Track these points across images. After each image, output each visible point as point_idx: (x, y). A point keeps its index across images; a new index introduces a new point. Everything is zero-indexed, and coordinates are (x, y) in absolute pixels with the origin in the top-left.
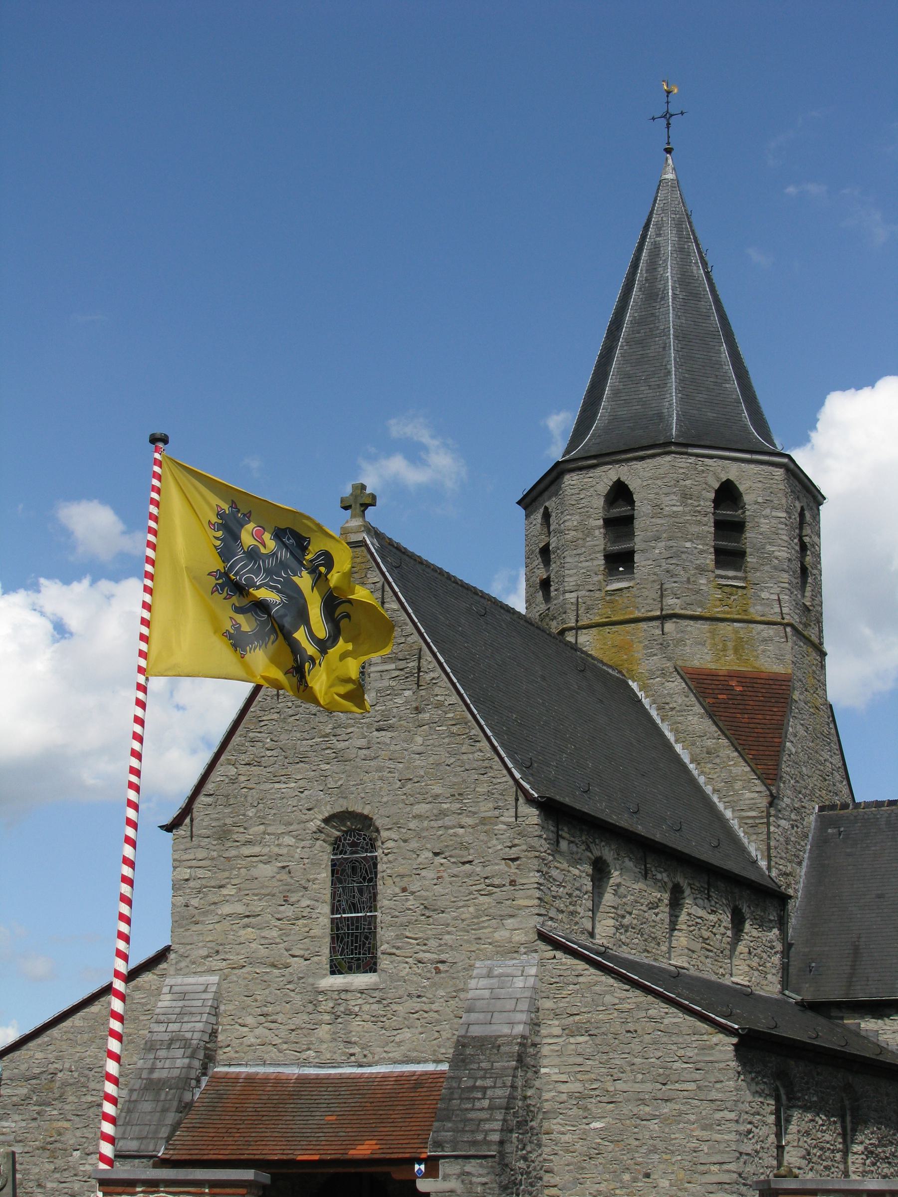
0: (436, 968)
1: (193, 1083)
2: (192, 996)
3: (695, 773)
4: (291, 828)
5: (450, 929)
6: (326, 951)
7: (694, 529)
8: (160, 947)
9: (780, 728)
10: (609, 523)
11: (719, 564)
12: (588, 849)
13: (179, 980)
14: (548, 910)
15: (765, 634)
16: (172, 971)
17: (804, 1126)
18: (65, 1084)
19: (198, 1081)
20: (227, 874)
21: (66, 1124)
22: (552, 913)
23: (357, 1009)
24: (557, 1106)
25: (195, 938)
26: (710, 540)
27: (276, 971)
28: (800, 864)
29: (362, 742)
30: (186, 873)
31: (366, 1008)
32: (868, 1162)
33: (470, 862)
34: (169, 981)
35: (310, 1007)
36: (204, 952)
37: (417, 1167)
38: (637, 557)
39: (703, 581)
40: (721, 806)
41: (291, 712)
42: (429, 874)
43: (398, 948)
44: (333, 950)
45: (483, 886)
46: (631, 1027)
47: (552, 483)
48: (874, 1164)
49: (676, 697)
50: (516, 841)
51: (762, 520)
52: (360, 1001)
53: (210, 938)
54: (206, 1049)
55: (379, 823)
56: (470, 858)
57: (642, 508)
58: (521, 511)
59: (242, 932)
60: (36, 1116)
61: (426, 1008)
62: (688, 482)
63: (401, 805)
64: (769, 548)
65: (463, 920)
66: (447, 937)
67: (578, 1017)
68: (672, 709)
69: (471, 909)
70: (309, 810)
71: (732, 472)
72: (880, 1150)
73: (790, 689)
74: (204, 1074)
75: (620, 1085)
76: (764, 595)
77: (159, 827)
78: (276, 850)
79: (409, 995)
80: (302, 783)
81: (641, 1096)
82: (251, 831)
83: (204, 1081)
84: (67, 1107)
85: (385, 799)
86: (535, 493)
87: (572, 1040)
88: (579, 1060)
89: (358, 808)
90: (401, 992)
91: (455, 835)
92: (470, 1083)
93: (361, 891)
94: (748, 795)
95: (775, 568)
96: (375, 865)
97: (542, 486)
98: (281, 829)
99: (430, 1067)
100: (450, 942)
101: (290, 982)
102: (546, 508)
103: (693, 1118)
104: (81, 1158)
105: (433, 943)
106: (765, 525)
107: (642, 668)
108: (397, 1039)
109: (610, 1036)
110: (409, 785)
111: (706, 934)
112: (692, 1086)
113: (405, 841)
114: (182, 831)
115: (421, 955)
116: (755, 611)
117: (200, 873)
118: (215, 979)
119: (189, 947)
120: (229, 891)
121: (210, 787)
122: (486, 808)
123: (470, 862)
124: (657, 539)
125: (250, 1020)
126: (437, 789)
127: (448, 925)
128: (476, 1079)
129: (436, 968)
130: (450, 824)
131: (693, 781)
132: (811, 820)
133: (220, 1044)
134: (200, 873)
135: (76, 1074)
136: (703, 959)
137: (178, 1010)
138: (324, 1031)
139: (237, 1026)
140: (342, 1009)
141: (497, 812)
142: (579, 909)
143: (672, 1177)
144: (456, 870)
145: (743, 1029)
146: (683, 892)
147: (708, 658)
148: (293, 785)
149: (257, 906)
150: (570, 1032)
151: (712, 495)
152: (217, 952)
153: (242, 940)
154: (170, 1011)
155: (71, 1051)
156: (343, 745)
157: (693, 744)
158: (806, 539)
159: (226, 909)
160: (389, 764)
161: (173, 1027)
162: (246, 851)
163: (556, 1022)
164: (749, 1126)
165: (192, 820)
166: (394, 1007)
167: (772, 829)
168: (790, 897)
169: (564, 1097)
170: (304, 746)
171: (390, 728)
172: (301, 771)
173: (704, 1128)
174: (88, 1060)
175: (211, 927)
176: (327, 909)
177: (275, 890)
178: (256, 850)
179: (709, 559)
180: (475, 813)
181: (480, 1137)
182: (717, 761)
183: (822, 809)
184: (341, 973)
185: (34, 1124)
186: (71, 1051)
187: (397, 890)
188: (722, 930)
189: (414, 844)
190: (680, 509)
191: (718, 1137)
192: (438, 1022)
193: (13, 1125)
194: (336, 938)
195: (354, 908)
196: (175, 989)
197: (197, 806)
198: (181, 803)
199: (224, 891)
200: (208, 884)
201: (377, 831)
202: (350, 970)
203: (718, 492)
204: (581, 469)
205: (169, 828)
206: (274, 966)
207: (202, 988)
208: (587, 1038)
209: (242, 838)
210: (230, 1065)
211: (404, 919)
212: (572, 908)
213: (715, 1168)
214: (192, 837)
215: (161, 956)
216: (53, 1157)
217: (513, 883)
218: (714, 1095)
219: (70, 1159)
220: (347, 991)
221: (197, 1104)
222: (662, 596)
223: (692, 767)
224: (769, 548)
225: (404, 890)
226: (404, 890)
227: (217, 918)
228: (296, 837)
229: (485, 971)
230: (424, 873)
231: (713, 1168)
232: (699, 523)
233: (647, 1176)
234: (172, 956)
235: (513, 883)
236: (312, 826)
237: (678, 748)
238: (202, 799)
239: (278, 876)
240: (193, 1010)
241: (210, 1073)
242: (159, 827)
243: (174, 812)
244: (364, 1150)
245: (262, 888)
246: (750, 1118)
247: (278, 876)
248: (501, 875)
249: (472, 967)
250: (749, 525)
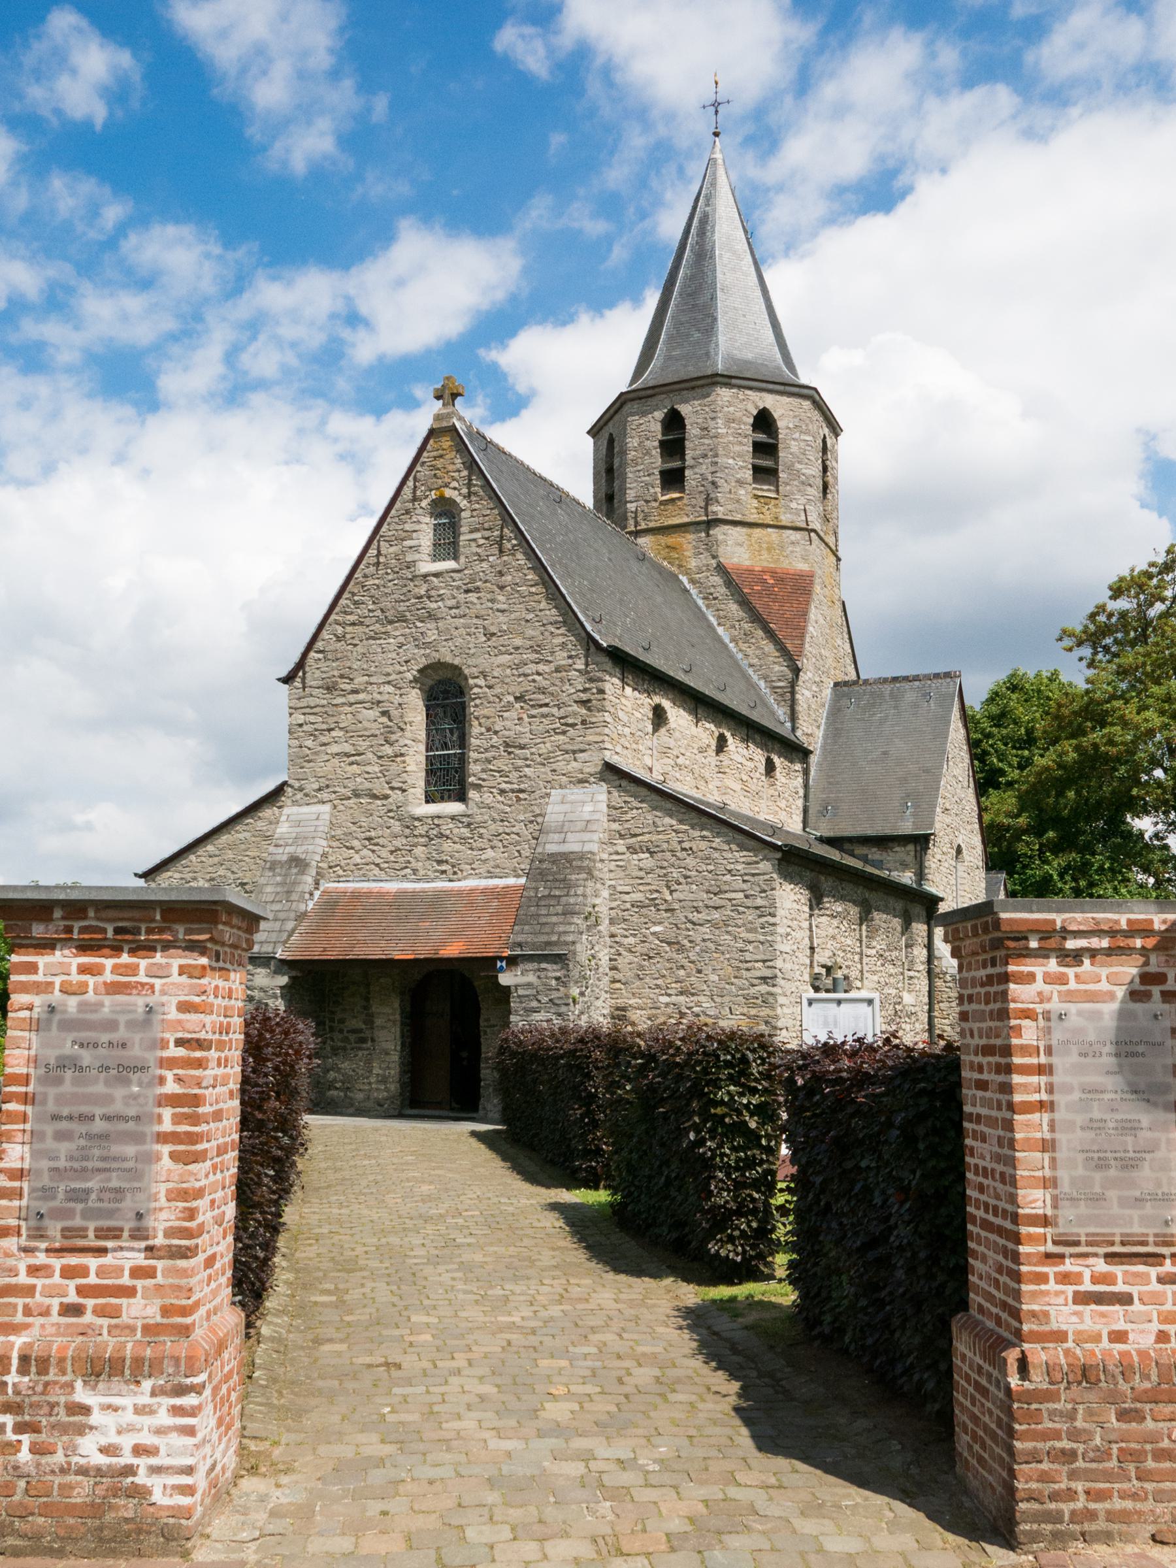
0: (517, 797)
1: (307, 896)
3: (735, 650)
4: (391, 678)
5: (528, 762)
6: (422, 783)
7: (737, 448)
8: (279, 782)
9: (804, 614)
10: (663, 444)
11: (756, 480)
12: (649, 696)
13: (295, 809)
14: (614, 746)
15: (793, 538)
16: (289, 802)
17: (831, 931)
19: (311, 894)
20: (335, 719)
22: (619, 749)
23: (448, 832)
24: (620, 914)
26: (749, 458)
27: (379, 802)
28: (818, 727)
29: (452, 603)
30: (301, 719)
31: (456, 831)
32: (879, 963)
33: (546, 705)
34: (286, 811)
35: (407, 831)
36: (316, 786)
37: (499, 964)
38: (687, 473)
39: (742, 492)
40: (755, 678)
41: (390, 577)
42: (513, 714)
43: (484, 780)
44: (428, 783)
45: (558, 725)
46: (686, 845)
47: (616, 412)
48: (883, 965)
49: (719, 589)
50: (587, 686)
51: (793, 442)
52: (451, 826)
54: (318, 867)
55: (466, 671)
56: (547, 701)
57: (692, 430)
58: (590, 441)
59: (349, 768)
61: (507, 830)
62: (731, 409)
63: (487, 656)
64: (798, 466)
65: (540, 755)
66: (526, 769)
67: (639, 838)
68: (715, 599)
69: (548, 745)
70: (406, 662)
71: (769, 401)
72: (887, 954)
73: (812, 583)
74: (317, 889)
75: (675, 895)
76: (794, 505)
77: (279, 680)
78: (379, 697)
79: (494, 820)
80: (401, 639)
81: (695, 904)
82: (356, 681)
83: (317, 894)
85: (472, 651)
86: (602, 423)
87: (635, 856)
88: (642, 874)
89: (449, 659)
90: (486, 817)
91: (534, 681)
92: (546, 893)
93: (451, 730)
94: (777, 668)
95: (803, 483)
96: (464, 709)
97: (608, 416)
98: (382, 679)
99: (511, 881)
100: (529, 774)
101: (390, 811)
102: (611, 435)
103: (740, 922)
105: (514, 775)
106: (794, 447)
107: (693, 563)
108: (483, 857)
109: (668, 854)
110: (494, 639)
111: (745, 778)
112: (741, 895)
113: (490, 687)
114: (297, 683)
115: (504, 786)
116: (785, 519)
118: (327, 808)
121: (319, 645)
122: (561, 658)
123: (546, 705)
124: (705, 456)
125: (356, 843)
126: (518, 642)
127: (526, 759)
128: (551, 889)
129: (517, 797)
130: (529, 671)
131: (731, 656)
132: (827, 692)
134: (312, 718)
136: (742, 798)
138: (419, 851)
140: (435, 832)
141: (570, 661)
142: (641, 748)
143: (721, 972)
144: (534, 712)
145: (786, 846)
146: (726, 741)
147: (746, 556)
148: (392, 640)
149: (363, 745)
150: (632, 849)
151: (751, 420)
154: (287, 836)
156: (433, 605)
157: (733, 627)
158: (828, 463)
159: (334, 749)
160: (475, 621)
161: (289, 849)
162: (352, 698)
163: (622, 842)
164: (789, 930)
165: (304, 674)
166: (482, 831)
167: (798, 696)
168: (811, 752)
169: (628, 906)
170: (402, 607)
171: (477, 590)
172: (398, 630)
173: (749, 931)
176: (422, 747)
177: (378, 732)
178: (361, 696)
179: (748, 474)
180: (551, 662)
181: (554, 938)
182: (753, 641)
183: (836, 684)
184: (434, 802)
187: (483, 730)
188: (758, 775)
189: (497, 690)
190: (725, 431)
191: (762, 938)
192: (518, 843)
194: (430, 772)
195: (445, 746)
196: (291, 818)
197: (310, 661)
198: (296, 657)
199: (334, 734)
201: (466, 679)
202: (442, 799)
203: (756, 418)
204: (640, 399)
205: (287, 680)
206: (375, 797)
207: (315, 817)
208: (647, 855)
209: (348, 687)
211: (488, 755)
212: (634, 746)
213: (760, 965)
214: (304, 688)
215: (278, 791)
217: (584, 722)
218: (759, 902)
220: (439, 817)
222: (707, 505)
223: (731, 645)
224: (798, 466)
225: (489, 730)
226: (489, 730)
227: (326, 757)
228: (394, 686)
229: (559, 798)
230: (505, 714)
231: (757, 965)
232: (741, 443)
233: (699, 972)
235: (584, 722)
236: (409, 676)
237: (720, 630)
238: (312, 654)
239: (380, 720)
240: (307, 835)
241: (322, 889)
242: (279, 680)
243: (291, 666)
244: (453, 950)
245: (366, 729)
246: (790, 923)
247: (380, 720)
248: (575, 714)
249: (548, 795)
250: (781, 446)
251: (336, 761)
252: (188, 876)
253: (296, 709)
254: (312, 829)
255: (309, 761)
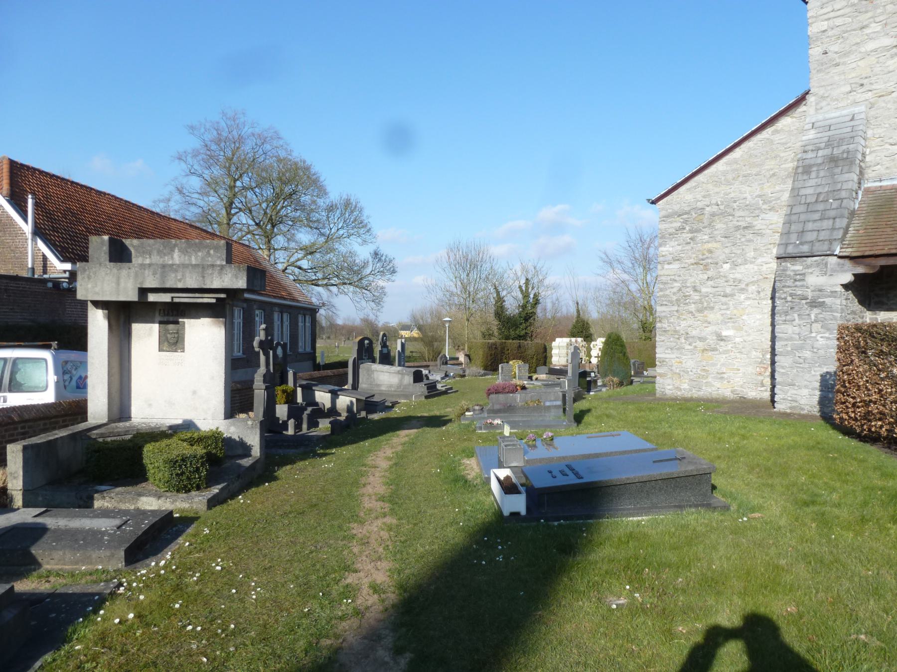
2: (838, 126)
18: (713, 215)
20: (870, 14)
21: (715, 245)
25: (837, 78)
53: (853, 75)
59: (890, 62)
60: (689, 241)
83: (860, 193)
84: (716, 232)
104: (731, 269)
117: (838, 22)
119: (829, 88)
120: (875, 28)
133: (868, 164)
134: (838, 22)
135: (722, 207)
137: (826, 139)
139: (887, 146)
152: (862, 85)
153: (891, 68)
155: (717, 190)
159: (871, 46)
174: (732, 195)
175: (854, 65)
185: (688, 247)
186: (717, 190)
193: (671, 249)
199: (867, 31)
200: (849, 29)
210: (881, 181)
216: (706, 268)
219: (721, 270)
221: (859, 212)
234: (810, 99)
241: (862, 188)
251: (872, 59)
252: (699, 197)
253: (816, 17)
254: (849, 129)
255: (837, 65)
